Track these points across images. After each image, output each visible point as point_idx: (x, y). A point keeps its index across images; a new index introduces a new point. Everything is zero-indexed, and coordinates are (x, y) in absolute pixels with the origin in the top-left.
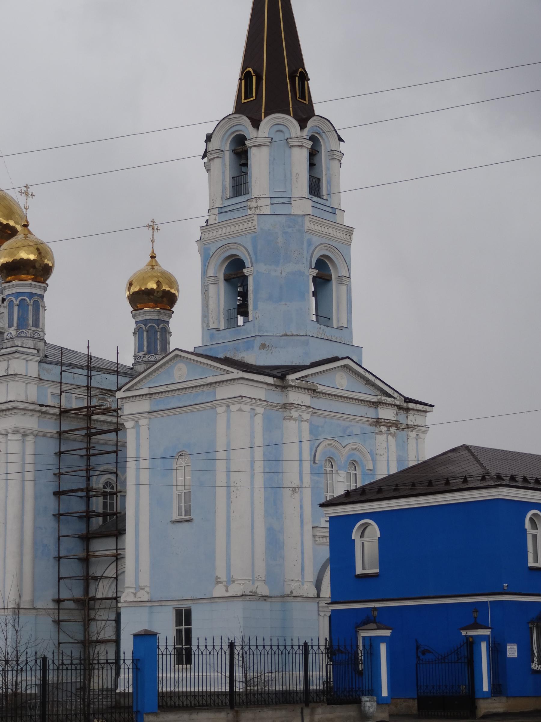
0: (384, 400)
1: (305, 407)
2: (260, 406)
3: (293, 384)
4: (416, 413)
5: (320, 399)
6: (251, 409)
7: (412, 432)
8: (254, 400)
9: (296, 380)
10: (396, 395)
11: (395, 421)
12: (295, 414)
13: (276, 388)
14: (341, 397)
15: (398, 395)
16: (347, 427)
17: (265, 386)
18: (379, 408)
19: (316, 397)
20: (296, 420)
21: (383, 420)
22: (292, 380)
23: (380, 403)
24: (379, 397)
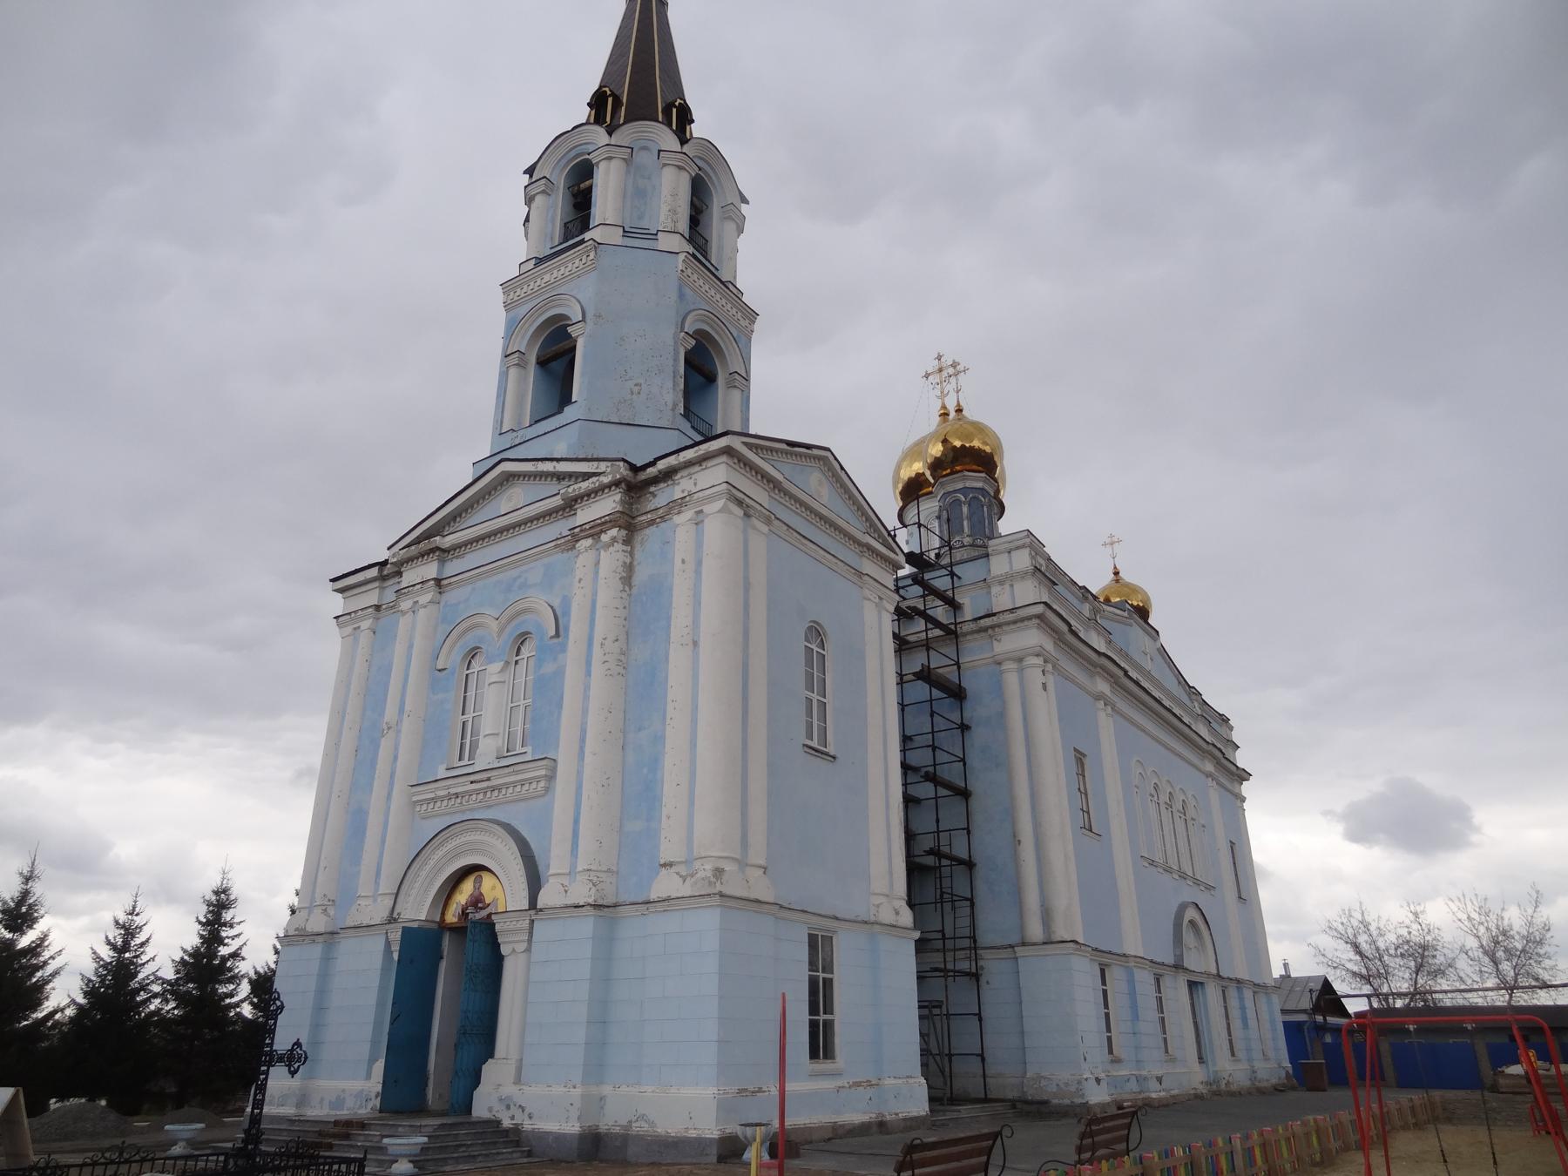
2: (362, 619)
4: (697, 468)
6: (355, 629)
7: (681, 515)
9: (401, 552)
10: (603, 466)
11: (607, 518)
15: (609, 464)
16: (515, 579)
17: (376, 584)
19: (457, 557)
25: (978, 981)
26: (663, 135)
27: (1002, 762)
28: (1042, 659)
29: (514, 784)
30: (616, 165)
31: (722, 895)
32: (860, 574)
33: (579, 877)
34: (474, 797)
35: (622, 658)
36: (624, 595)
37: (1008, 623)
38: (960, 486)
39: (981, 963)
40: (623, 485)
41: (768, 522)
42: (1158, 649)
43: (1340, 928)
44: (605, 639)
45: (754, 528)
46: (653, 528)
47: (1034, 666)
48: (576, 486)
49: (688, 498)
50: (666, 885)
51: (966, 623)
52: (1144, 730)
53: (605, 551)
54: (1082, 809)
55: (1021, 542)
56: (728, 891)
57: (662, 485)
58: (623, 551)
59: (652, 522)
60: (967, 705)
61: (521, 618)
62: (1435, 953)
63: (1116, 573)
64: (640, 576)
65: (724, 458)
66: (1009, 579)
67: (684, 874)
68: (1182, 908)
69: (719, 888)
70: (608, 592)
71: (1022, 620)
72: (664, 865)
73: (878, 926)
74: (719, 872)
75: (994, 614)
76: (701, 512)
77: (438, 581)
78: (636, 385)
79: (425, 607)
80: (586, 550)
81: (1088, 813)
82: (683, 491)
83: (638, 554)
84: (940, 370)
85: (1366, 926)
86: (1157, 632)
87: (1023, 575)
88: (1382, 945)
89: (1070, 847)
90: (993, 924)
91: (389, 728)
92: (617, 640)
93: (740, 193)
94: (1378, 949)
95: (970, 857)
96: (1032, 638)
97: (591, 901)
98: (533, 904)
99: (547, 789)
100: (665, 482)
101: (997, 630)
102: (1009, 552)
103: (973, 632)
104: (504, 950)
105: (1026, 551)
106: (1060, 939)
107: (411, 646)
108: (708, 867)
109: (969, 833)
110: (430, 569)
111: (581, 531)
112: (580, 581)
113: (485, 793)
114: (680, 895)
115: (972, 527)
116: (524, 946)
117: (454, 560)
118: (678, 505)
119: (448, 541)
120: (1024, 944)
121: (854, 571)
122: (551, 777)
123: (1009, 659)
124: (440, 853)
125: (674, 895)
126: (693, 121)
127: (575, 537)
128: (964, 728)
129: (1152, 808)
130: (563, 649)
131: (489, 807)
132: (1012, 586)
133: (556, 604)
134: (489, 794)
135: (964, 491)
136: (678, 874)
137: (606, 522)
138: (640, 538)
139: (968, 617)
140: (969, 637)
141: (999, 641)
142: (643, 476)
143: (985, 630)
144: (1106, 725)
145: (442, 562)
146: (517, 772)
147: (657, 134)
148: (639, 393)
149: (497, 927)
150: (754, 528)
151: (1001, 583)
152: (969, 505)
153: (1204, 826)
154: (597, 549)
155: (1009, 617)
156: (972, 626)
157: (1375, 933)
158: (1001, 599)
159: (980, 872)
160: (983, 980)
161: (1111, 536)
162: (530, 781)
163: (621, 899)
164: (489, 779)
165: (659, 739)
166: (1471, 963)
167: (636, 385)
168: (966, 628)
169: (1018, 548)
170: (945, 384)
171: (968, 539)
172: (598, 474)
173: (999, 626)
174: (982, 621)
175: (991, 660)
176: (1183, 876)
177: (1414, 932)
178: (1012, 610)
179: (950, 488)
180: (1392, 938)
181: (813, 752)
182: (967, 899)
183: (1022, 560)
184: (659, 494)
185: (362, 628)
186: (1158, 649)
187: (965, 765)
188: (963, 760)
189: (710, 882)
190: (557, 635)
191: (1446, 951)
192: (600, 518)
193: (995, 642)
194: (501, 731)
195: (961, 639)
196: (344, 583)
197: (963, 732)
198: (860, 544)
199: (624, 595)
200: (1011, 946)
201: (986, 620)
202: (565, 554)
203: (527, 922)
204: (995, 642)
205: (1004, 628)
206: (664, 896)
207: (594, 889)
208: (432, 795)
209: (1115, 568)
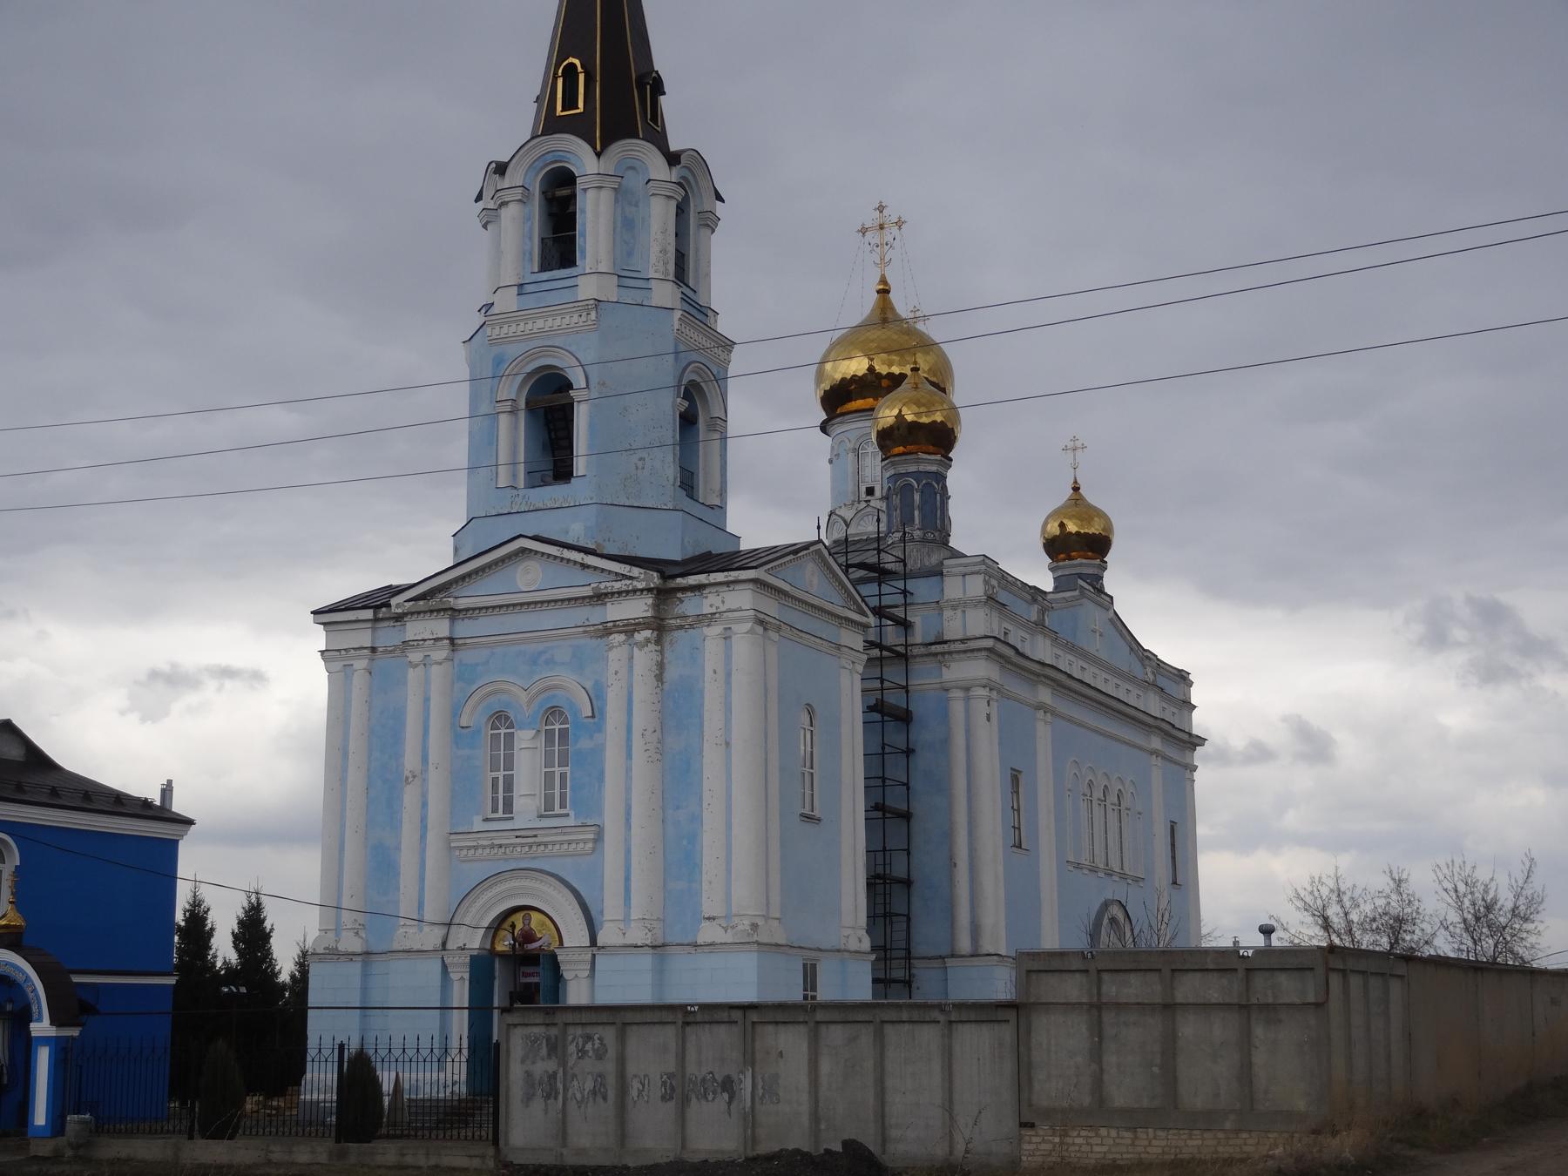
0: (606, 587)
1: (432, 641)
2: (359, 657)
3: (400, 611)
4: (725, 588)
5: (480, 618)
6: (345, 665)
8: (343, 652)
9: (406, 604)
10: (636, 571)
11: (641, 620)
12: (415, 656)
13: (397, 621)
14: (514, 605)
15: (642, 571)
16: (541, 653)
17: (369, 625)
18: (609, 604)
19: (470, 618)
20: (416, 666)
21: (609, 625)
22: (398, 606)
23: (606, 594)
24: (595, 585)
25: (910, 987)
26: (649, 154)
27: (943, 787)
28: (988, 689)
29: (561, 843)
30: (606, 196)
31: (759, 944)
32: (839, 646)
33: (633, 924)
34: (519, 849)
35: (659, 746)
36: (658, 690)
37: (958, 652)
38: (912, 468)
39: (913, 971)
40: (655, 592)
41: (778, 629)
42: (1111, 620)
43: (1309, 899)
44: (645, 730)
45: (770, 639)
46: (681, 632)
47: (981, 697)
48: (608, 584)
49: (717, 615)
50: (708, 933)
51: (917, 647)
52: (1081, 725)
53: (640, 650)
54: (1014, 827)
55: (976, 568)
56: (761, 940)
57: (689, 594)
58: (656, 651)
59: (681, 627)
60: (914, 728)
61: (551, 693)
62: (1413, 928)
63: (1076, 489)
64: (671, 673)
65: (751, 586)
66: (960, 605)
67: (725, 925)
68: (1106, 905)
69: (755, 938)
70: (643, 690)
71: (972, 651)
72: (709, 918)
73: (848, 954)
74: (754, 926)
75: (945, 642)
76: (730, 628)
77: (452, 640)
78: (640, 459)
79: (440, 664)
80: (620, 645)
81: (1019, 829)
82: (711, 606)
83: (668, 654)
84: (881, 227)
85: (1340, 894)
86: (1112, 598)
87: (976, 603)
88: (1354, 917)
89: (1001, 868)
90: (926, 936)
91: (414, 777)
92: (655, 731)
93: (715, 188)
94: (1349, 923)
95: (909, 876)
96: (978, 669)
97: (648, 942)
98: (593, 942)
99: (594, 850)
100: (692, 592)
101: (946, 656)
102: (964, 576)
103: (922, 656)
104: (566, 975)
105: (981, 577)
106: (987, 953)
107: (427, 700)
108: (746, 922)
109: (909, 854)
110: (441, 627)
111: (614, 626)
112: (616, 673)
113: (531, 847)
114: (723, 942)
115: (923, 517)
116: (587, 973)
117: (466, 620)
118: (710, 619)
119: (462, 603)
120: (953, 956)
121: (834, 646)
122: (599, 838)
123: (957, 688)
124: (489, 894)
125: (718, 941)
126: (664, 93)
127: (606, 630)
128: (909, 752)
129: (1084, 806)
130: (600, 728)
131: (534, 858)
132: (964, 612)
133: (588, 685)
134: (534, 848)
135: (917, 475)
136: (720, 925)
137: (639, 624)
138: (668, 639)
139: (918, 639)
140: (918, 660)
141: (948, 667)
142: (672, 584)
143: (936, 655)
144: (1043, 732)
145: (453, 619)
146: (565, 834)
147: (644, 154)
148: (643, 468)
149: (559, 958)
150: (770, 639)
151: (954, 608)
152: (922, 492)
153: (1139, 813)
154: (630, 645)
155: (961, 647)
156: (923, 650)
157: (1348, 904)
158: (953, 626)
159: (915, 889)
160: (914, 985)
161: (1074, 439)
162: (577, 842)
163: (669, 940)
164: (535, 836)
165: (696, 819)
166: (1450, 939)
167: (640, 459)
168: (916, 651)
169: (973, 573)
170: (886, 248)
171: (918, 532)
172: (631, 578)
173: (950, 653)
174: (933, 647)
175: (938, 686)
176: (1109, 873)
177: (1393, 904)
178: (962, 641)
179: (902, 469)
180: (1367, 908)
181: (806, 819)
182: (904, 915)
183: (976, 587)
184: (686, 601)
185: (355, 667)
186: (1111, 620)
187: (908, 789)
188: (907, 785)
189: (749, 934)
190: (593, 716)
191: (1424, 926)
192: (634, 619)
193: (944, 669)
194: (538, 793)
195: (910, 660)
196: (328, 615)
197: (908, 757)
198: (841, 618)
199: (658, 690)
200: (942, 958)
201: (937, 646)
202: (594, 640)
203: (590, 955)
204: (944, 669)
205: (954, 656)
206: (709, 941)
207: (650, 934)
208: (475, 844)
209: (1076, 482)
